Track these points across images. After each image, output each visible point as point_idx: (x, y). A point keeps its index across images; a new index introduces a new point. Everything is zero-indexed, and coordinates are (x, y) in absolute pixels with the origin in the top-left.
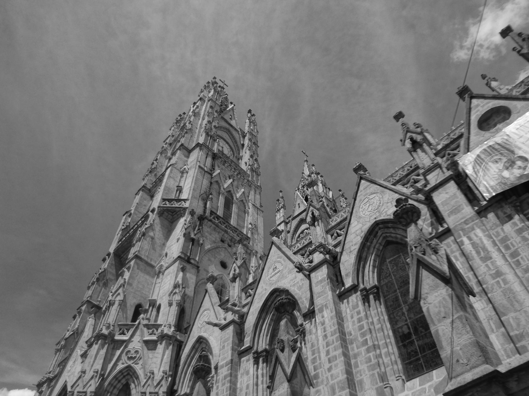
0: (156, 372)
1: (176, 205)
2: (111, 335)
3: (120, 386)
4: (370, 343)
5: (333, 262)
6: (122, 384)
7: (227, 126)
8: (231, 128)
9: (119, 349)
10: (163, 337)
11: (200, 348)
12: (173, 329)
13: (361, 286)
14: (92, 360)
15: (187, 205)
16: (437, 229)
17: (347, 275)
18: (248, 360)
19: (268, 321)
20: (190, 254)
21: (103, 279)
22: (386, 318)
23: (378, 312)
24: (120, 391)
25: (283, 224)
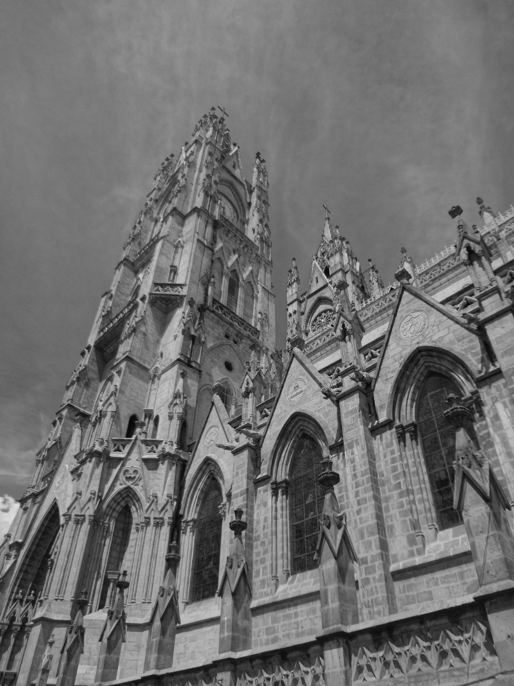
0: (159, 495)
1: (171, 292)
2: (106, 452)
3: (119, 508)
4: (403, 487)
5: (366, 389)
6: (121, 506)
7: (230, 178)
8: (234, 181)
9: (115, 468)
10: (165, 456)
11: (208, 471)
12: (175, 446)
13: (397, 423)
14: (87, 481)
15: (184, 292)
16: (488, 368)
17: (381, 407)
18: (265, 491)
19: (288, 447)
20: (191, 356)
21: (85, 379)
22: (423, 460)
23: (414, 454)
24: (120, 513)
25: (296, 303)
